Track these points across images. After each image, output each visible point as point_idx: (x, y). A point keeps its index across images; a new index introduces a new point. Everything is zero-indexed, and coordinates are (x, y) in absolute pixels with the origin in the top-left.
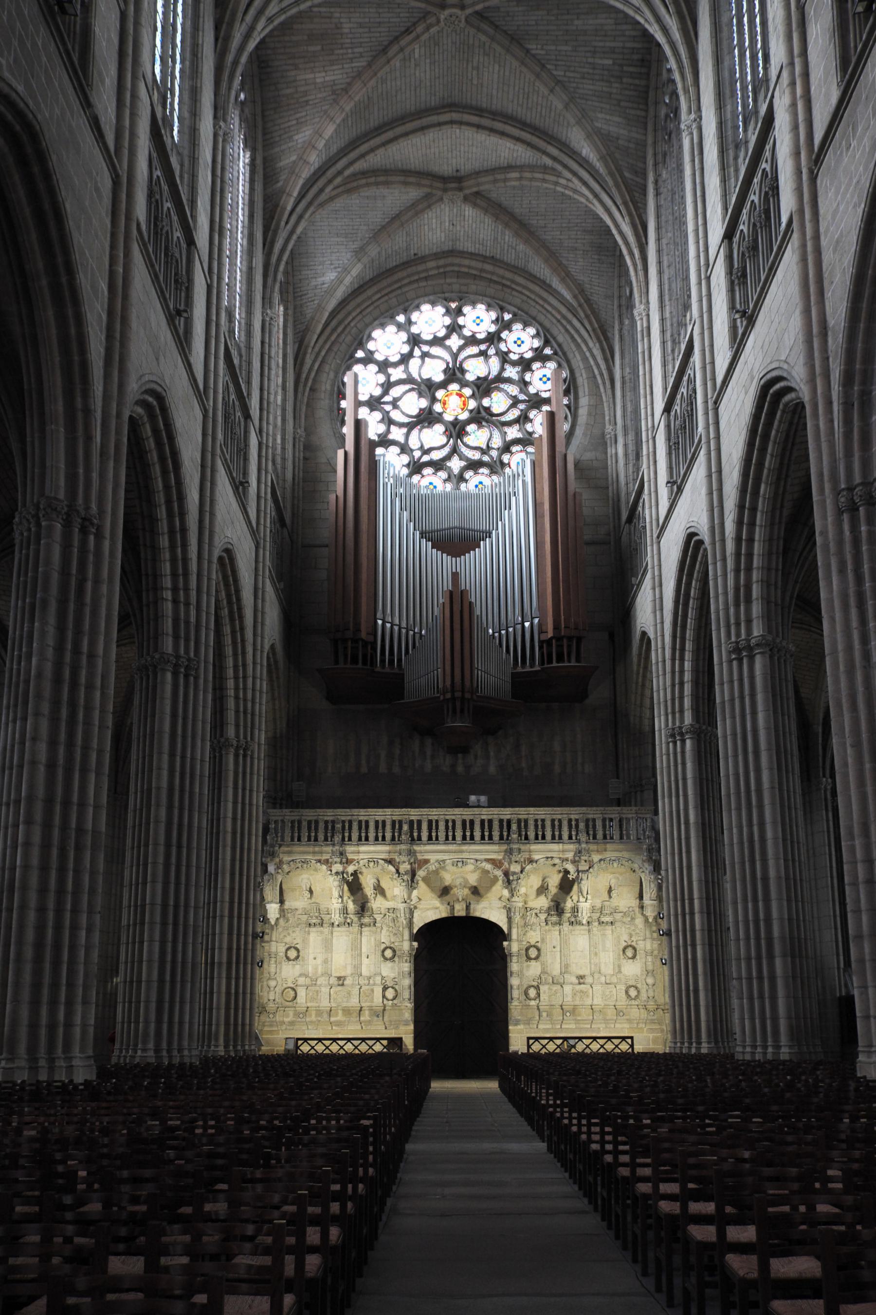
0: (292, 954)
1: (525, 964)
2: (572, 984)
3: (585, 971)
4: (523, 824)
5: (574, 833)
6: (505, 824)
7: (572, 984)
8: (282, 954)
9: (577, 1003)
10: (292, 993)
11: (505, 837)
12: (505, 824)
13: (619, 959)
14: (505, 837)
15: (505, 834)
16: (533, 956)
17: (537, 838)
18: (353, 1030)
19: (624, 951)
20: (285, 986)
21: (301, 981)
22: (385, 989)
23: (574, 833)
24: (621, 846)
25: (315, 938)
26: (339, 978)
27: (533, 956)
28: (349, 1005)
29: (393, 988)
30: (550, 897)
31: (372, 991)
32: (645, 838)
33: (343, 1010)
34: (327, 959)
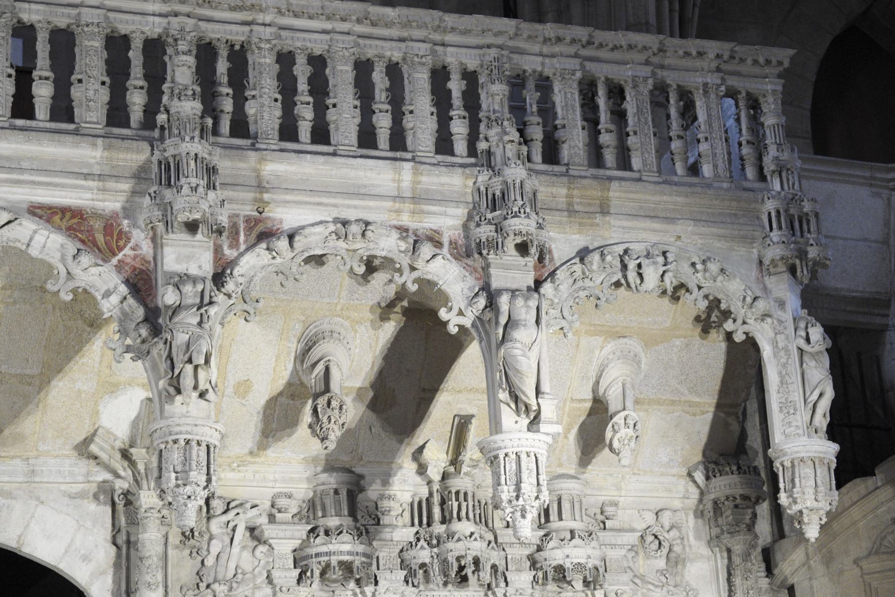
4: (222, 67)
5: (459, 129)
6: (136, 56)
11: (136, 114)
12: (136, 56)
14: (136, 114)
15: (137, 100)
17: (288, 132)
23: (459, 129)
24: (671, 199)
30: (335, 434)
32: (762, 177)
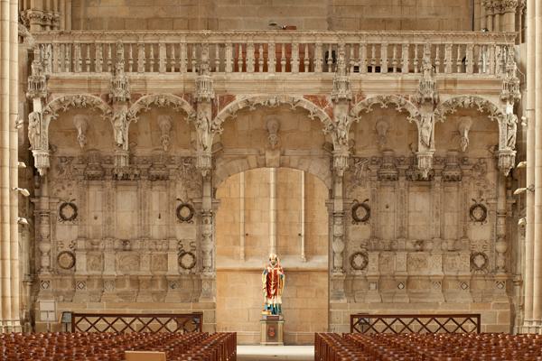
0: (68, 212)
1: (351, 227)
2: (406, 250)
3: (423, 236)
7: (406, 250)
8: (56, 213)
9: (412, 273)
10: (70, 259)
13: (465, 221)
16: (361, 217)
18: (143, 304)
19: (471, 212)
20: (61, 250)
21: (81, 244)
22: (182, 255)
25: (95, 193)
26: (125, 242)
27: (361, 217)
28: (140, 273)
29: (191, 254)
31: (166, 256)
33: (131, 280)
34: (110, 218)
